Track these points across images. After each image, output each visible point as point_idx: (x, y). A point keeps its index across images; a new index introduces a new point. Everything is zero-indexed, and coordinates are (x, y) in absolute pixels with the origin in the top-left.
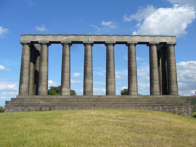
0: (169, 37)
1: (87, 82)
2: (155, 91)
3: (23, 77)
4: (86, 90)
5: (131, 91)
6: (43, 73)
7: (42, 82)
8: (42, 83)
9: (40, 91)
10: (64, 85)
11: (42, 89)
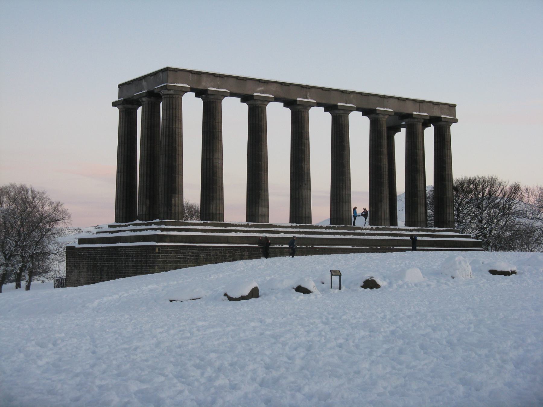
0: (444, 106)
1: (304, 195)
2: (419, 220)
3: (177, 176)
4: (304, 212)
5: (381, 219)
6: (217, 170)
7: (218, 191)
8: (218, 194)
9: (214, 212)
10: (260, 201)
11: (218, 208)
